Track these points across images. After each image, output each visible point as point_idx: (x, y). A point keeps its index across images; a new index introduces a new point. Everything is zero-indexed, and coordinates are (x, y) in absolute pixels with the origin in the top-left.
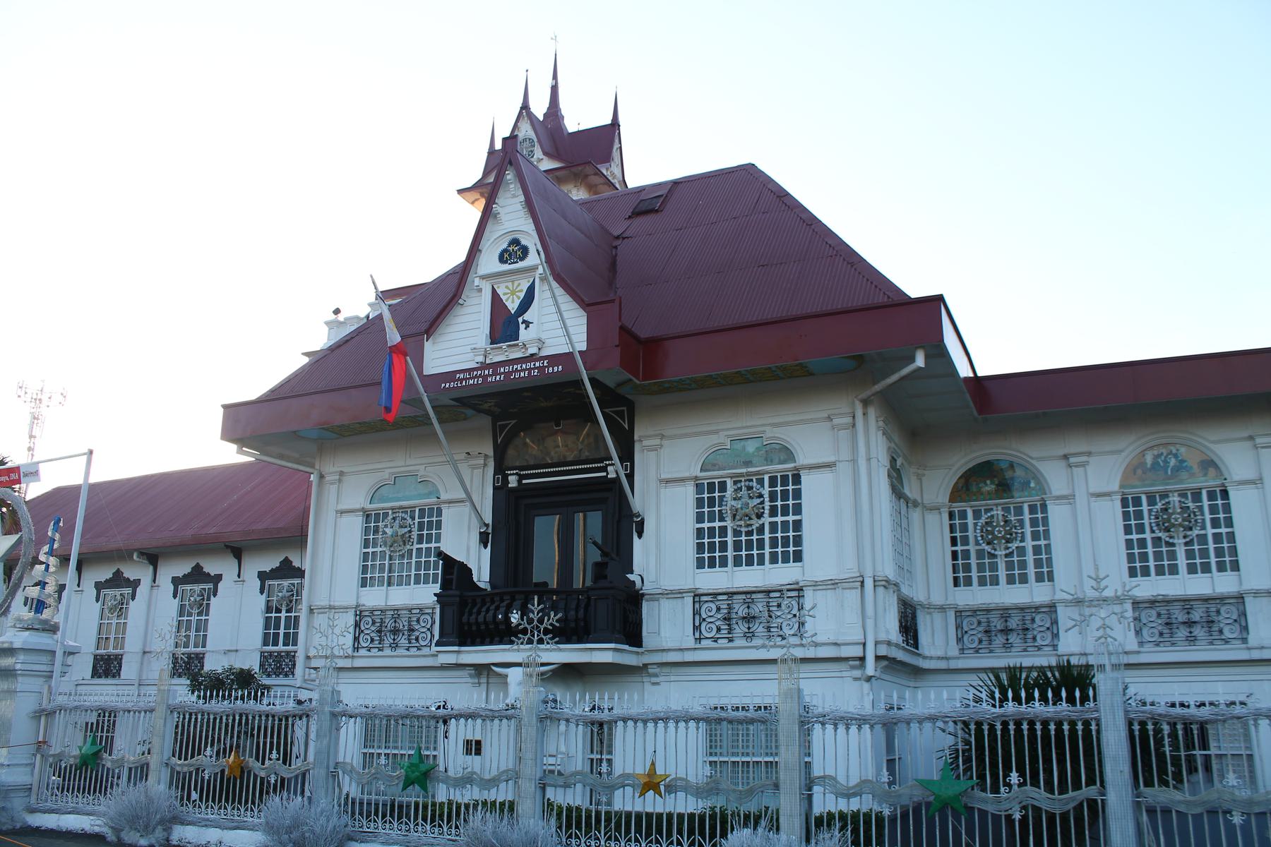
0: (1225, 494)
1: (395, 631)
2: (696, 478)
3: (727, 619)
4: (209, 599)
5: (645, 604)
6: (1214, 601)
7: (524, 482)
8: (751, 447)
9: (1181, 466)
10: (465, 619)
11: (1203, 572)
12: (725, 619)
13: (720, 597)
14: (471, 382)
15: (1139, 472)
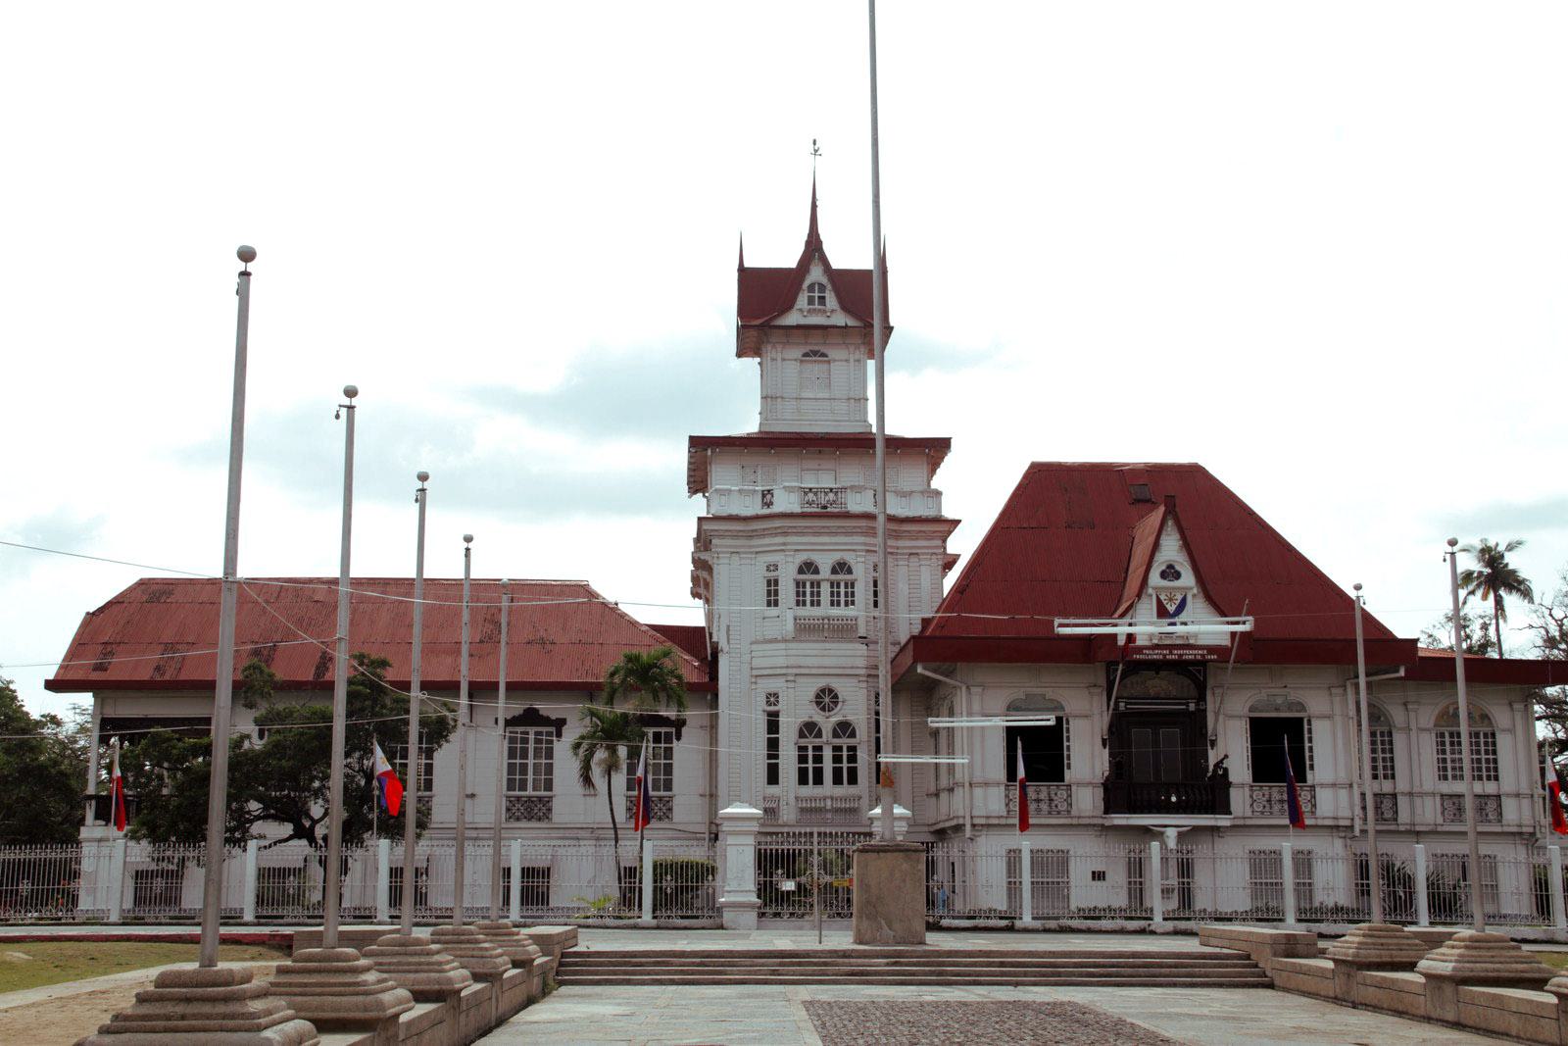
0: (1493, 735)
1: (1038, 801)
3: (1269, 801)
5: (1231, 789)
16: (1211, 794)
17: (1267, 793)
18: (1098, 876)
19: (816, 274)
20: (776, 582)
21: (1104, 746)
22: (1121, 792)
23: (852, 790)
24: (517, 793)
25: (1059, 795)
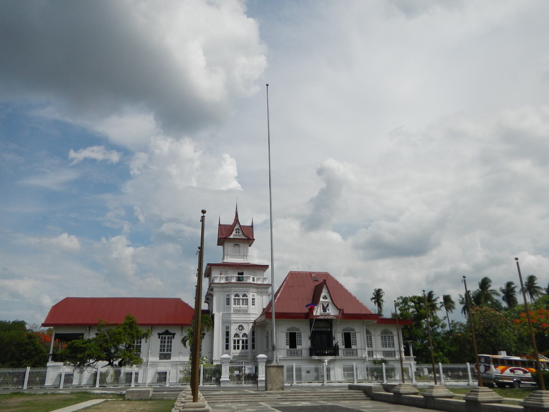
0: (393, 337)
1: (294, 353)
3: (347, 353)
4: (171, 339)
6: (392, 352)
9: (388, 332)
16: (334, 351)
18: (308, 372)
19: (237, 227)
20: (229, 299)
21: (309, 339)
22: (313, 351)
23: (246, 351)
24: (162, 352)
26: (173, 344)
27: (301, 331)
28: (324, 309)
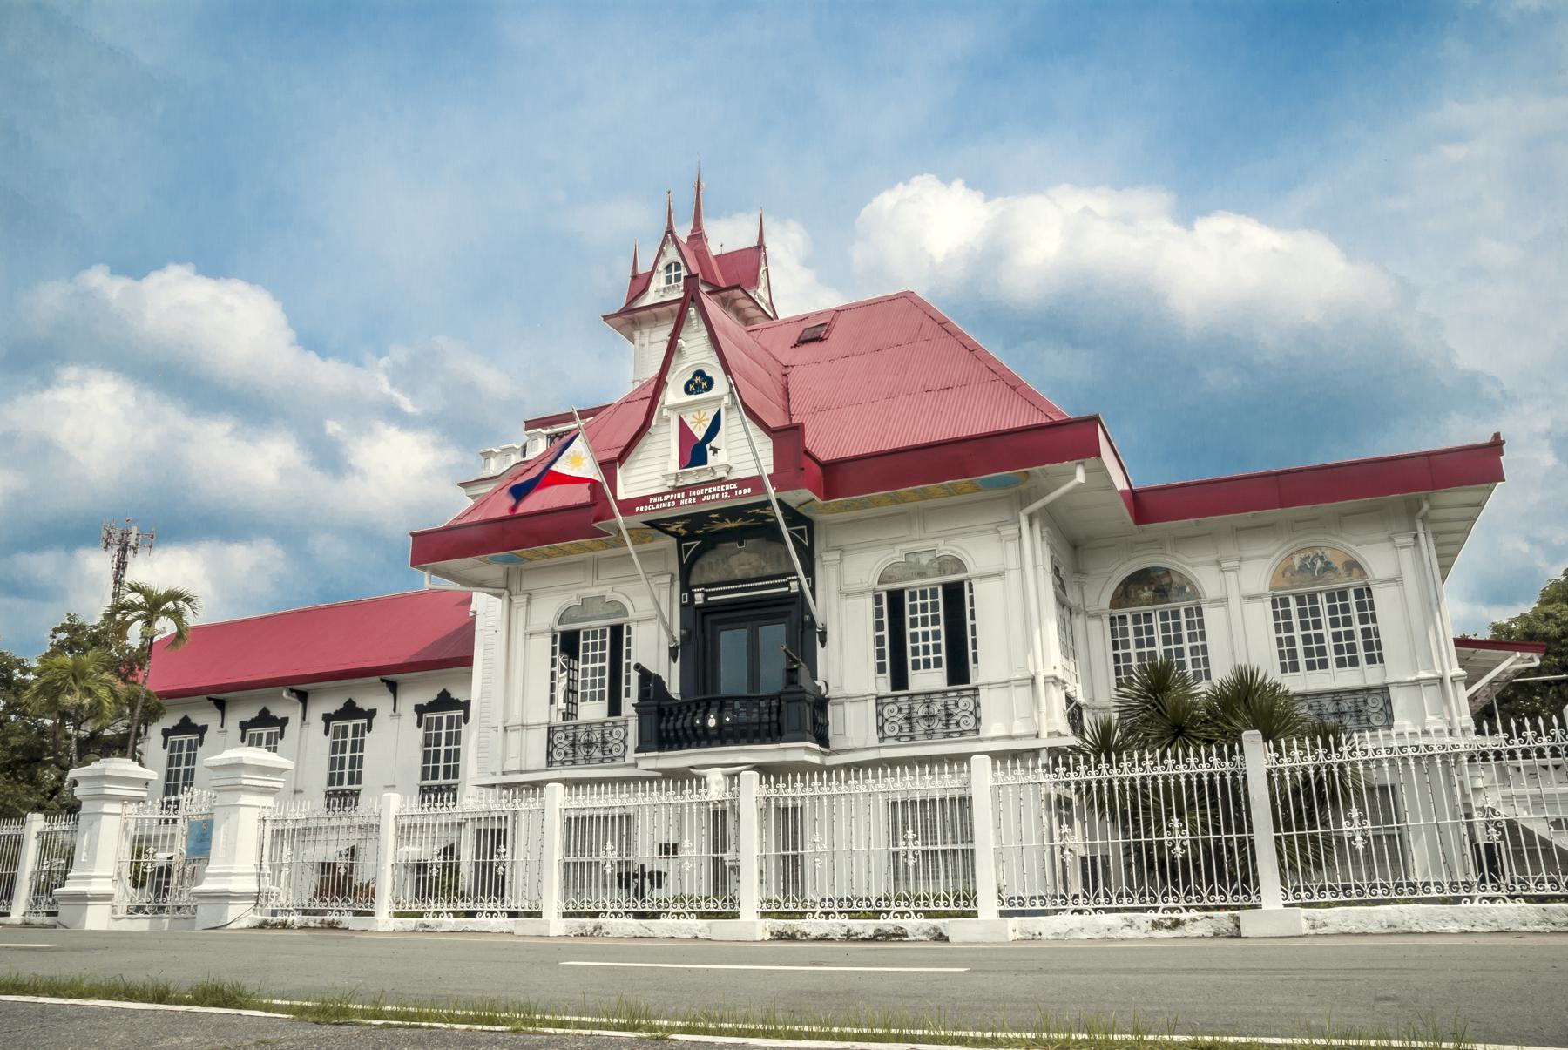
2: (874, 591)
7: (710, 599)
8: (925, 560)
9: (1328, 567)
10: (663, 726)
11: (1350, 665)
12: (906, 718)
13: (901, 699)
14: (665, 505)
15: (1288, 574)
17: (905, 707)
25: (615, 736)
26: (366, 754)
27: (632, 615)
28: (695, 452)
